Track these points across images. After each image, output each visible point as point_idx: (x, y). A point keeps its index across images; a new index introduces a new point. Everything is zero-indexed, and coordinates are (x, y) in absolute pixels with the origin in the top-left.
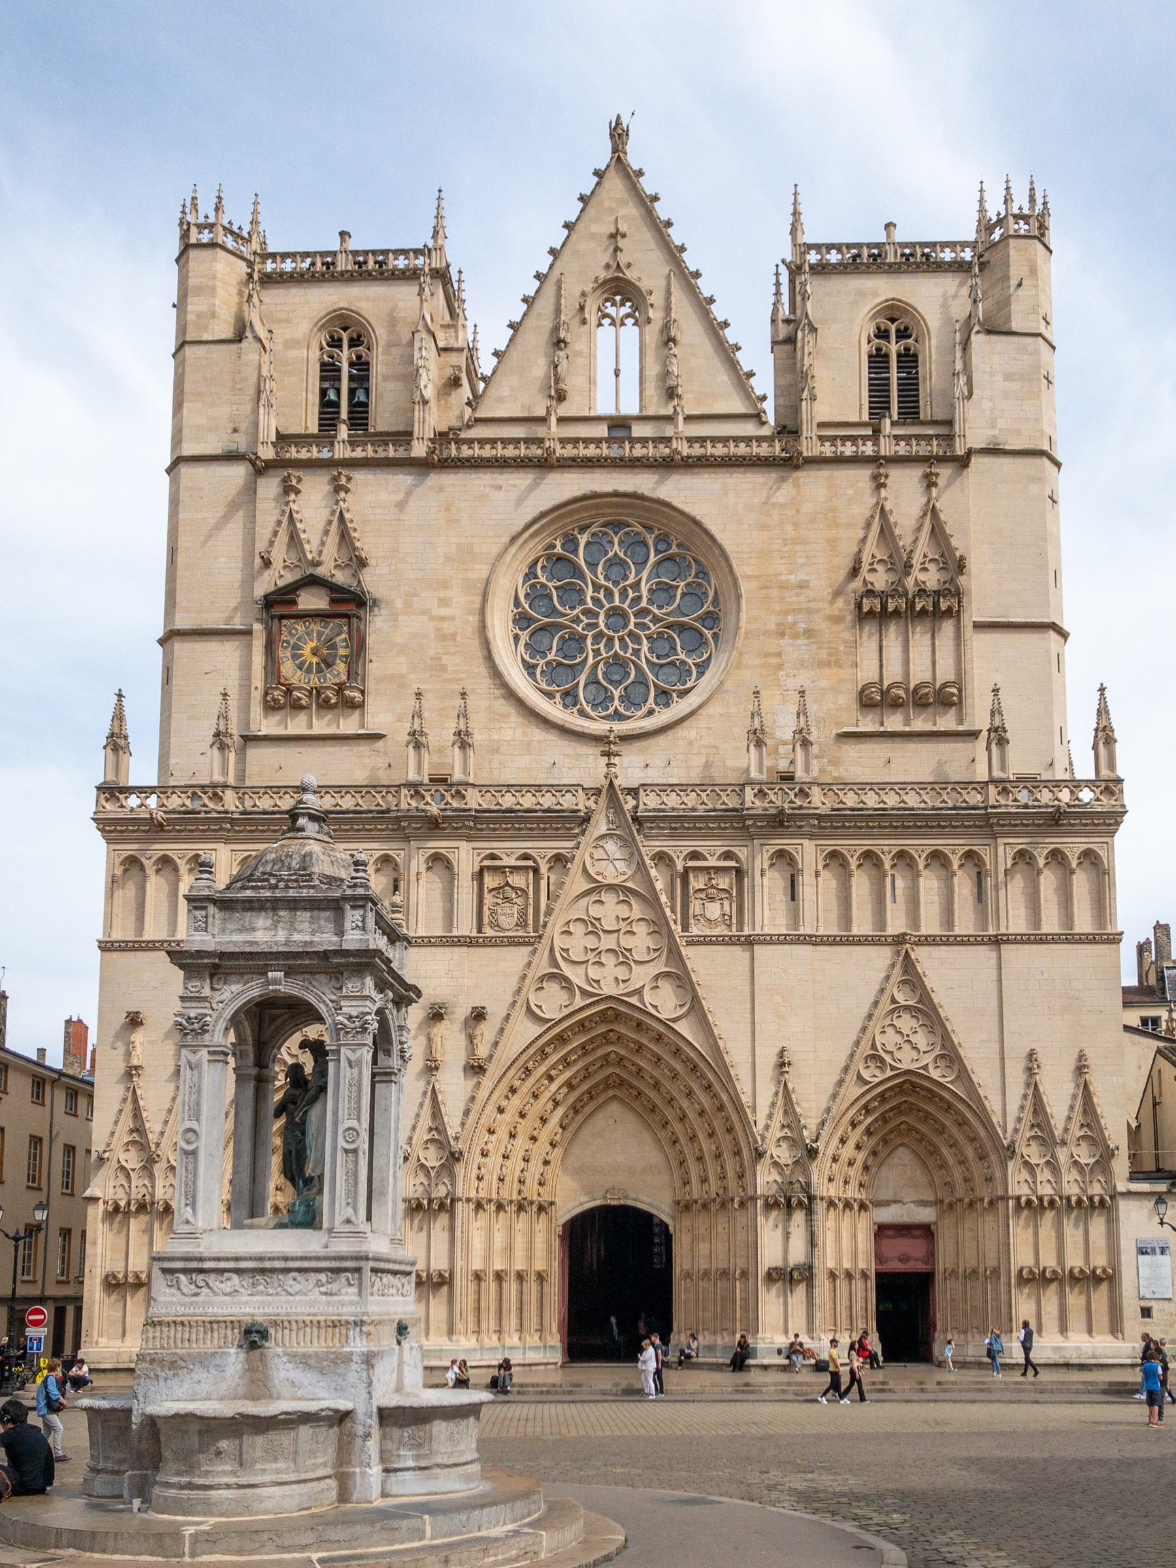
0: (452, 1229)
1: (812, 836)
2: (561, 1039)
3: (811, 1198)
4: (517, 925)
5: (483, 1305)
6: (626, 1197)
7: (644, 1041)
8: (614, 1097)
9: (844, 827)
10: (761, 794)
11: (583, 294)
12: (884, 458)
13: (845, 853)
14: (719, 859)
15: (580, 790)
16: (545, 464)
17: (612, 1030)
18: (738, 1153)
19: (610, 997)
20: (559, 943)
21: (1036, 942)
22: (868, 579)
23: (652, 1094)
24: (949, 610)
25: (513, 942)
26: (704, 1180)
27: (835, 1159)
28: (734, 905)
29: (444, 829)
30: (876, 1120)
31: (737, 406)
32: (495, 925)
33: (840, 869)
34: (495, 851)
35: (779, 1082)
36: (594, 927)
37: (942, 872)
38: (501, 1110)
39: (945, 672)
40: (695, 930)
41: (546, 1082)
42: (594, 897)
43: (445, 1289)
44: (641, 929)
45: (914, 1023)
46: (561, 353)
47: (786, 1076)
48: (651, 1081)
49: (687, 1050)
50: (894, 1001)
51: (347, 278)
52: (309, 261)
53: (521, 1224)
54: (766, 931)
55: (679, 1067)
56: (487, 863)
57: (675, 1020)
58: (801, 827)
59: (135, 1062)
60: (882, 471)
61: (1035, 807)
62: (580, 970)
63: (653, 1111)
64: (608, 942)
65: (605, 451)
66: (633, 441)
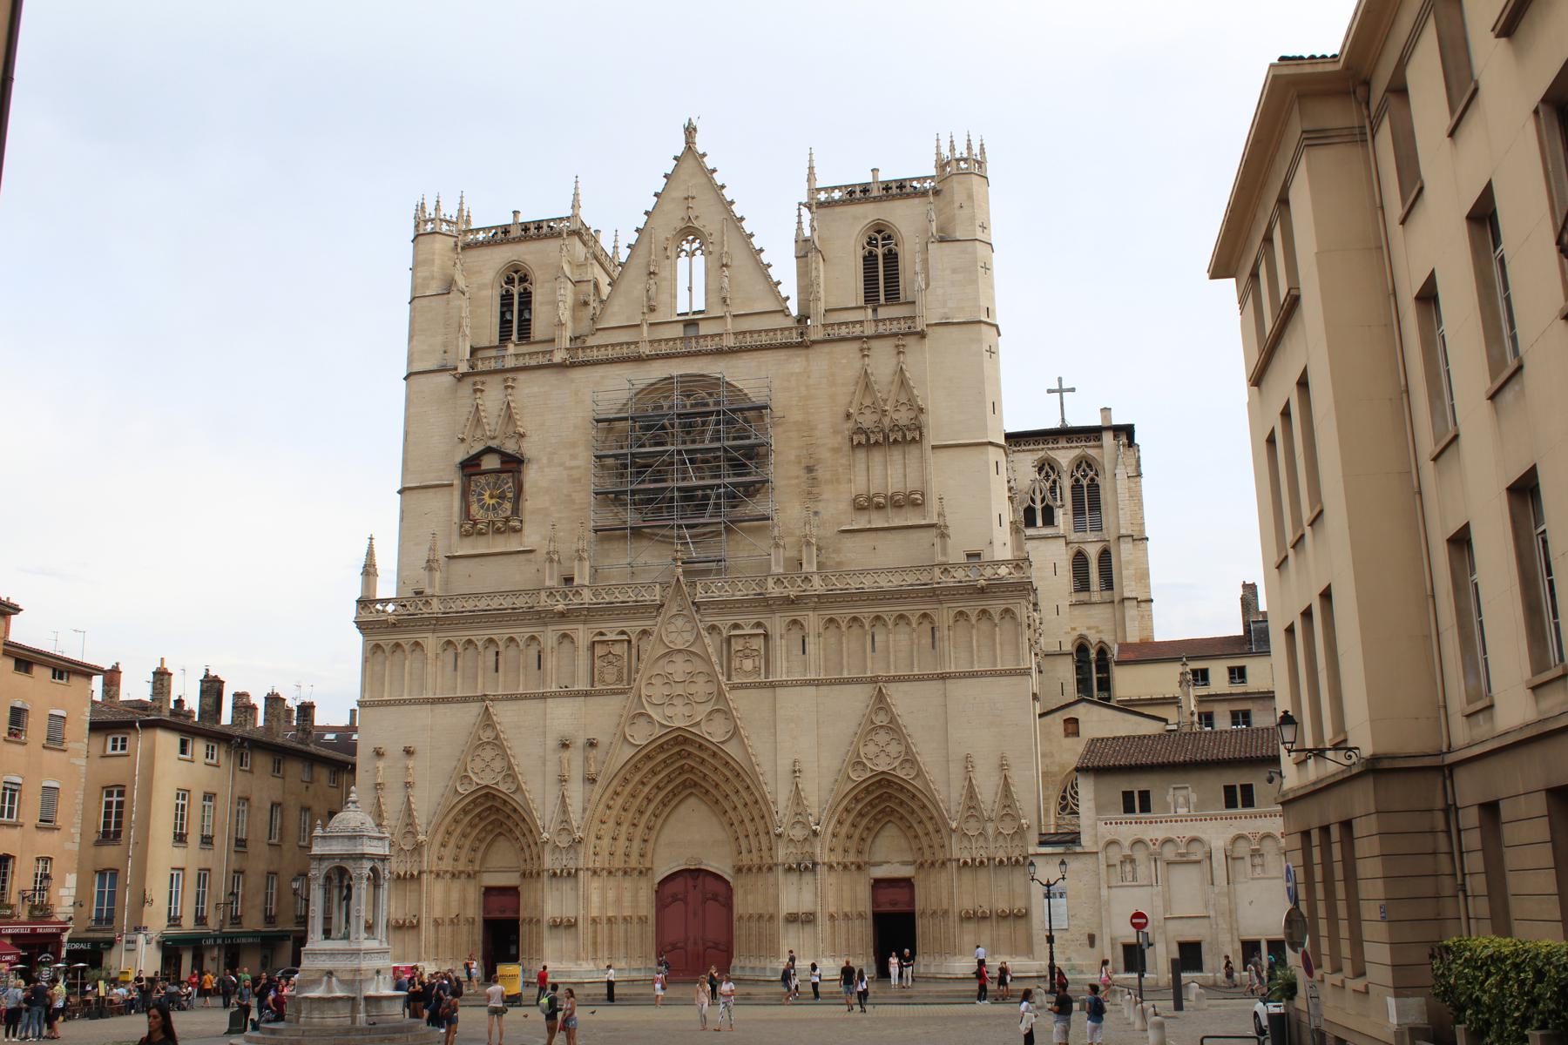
0: (577, 889)
1: (814, 609)
2: (648, 757)
3: (815, 864)
5: (599, 940)
6: (701, 863)
7: (705, 756)
8: (691, 794)
9: (836, 602)
10: (778, 581)
11: (667, 239)
12: (867, 337)
13: (838, 619)
14: (753, 627)
15: (658, 586)
16: (639, 359)
18: (768, 833)
20: (644, 692)
21: (969, 677)
22: (858, 420)
24: (914, 438)
25: (614, 693)
27: (834, 835)
30: (866, 805)
31: (771, 305)
32: (603, 681)
36: (668, 680)
37: (907, 629)
39: (913, 484)
40: (736, 680)
41: (641, 787)
42: (667, 660)
43: (573, 930)
44: (701, 680)
45: (888, 738)
46: (652, 282)
49: (732, 763)
50: (872, 722)
51: (519, 240)
52: (494, 231)
53: (627, 883)
55: (728, 774)
56: (597, 639)
57: (722, 743)
59: (379, 781)
60: (865, 346)
61: (966, 582)
62: (659, 710)
64: (679, 690)
65: (680, 348)
66: (697, 337)
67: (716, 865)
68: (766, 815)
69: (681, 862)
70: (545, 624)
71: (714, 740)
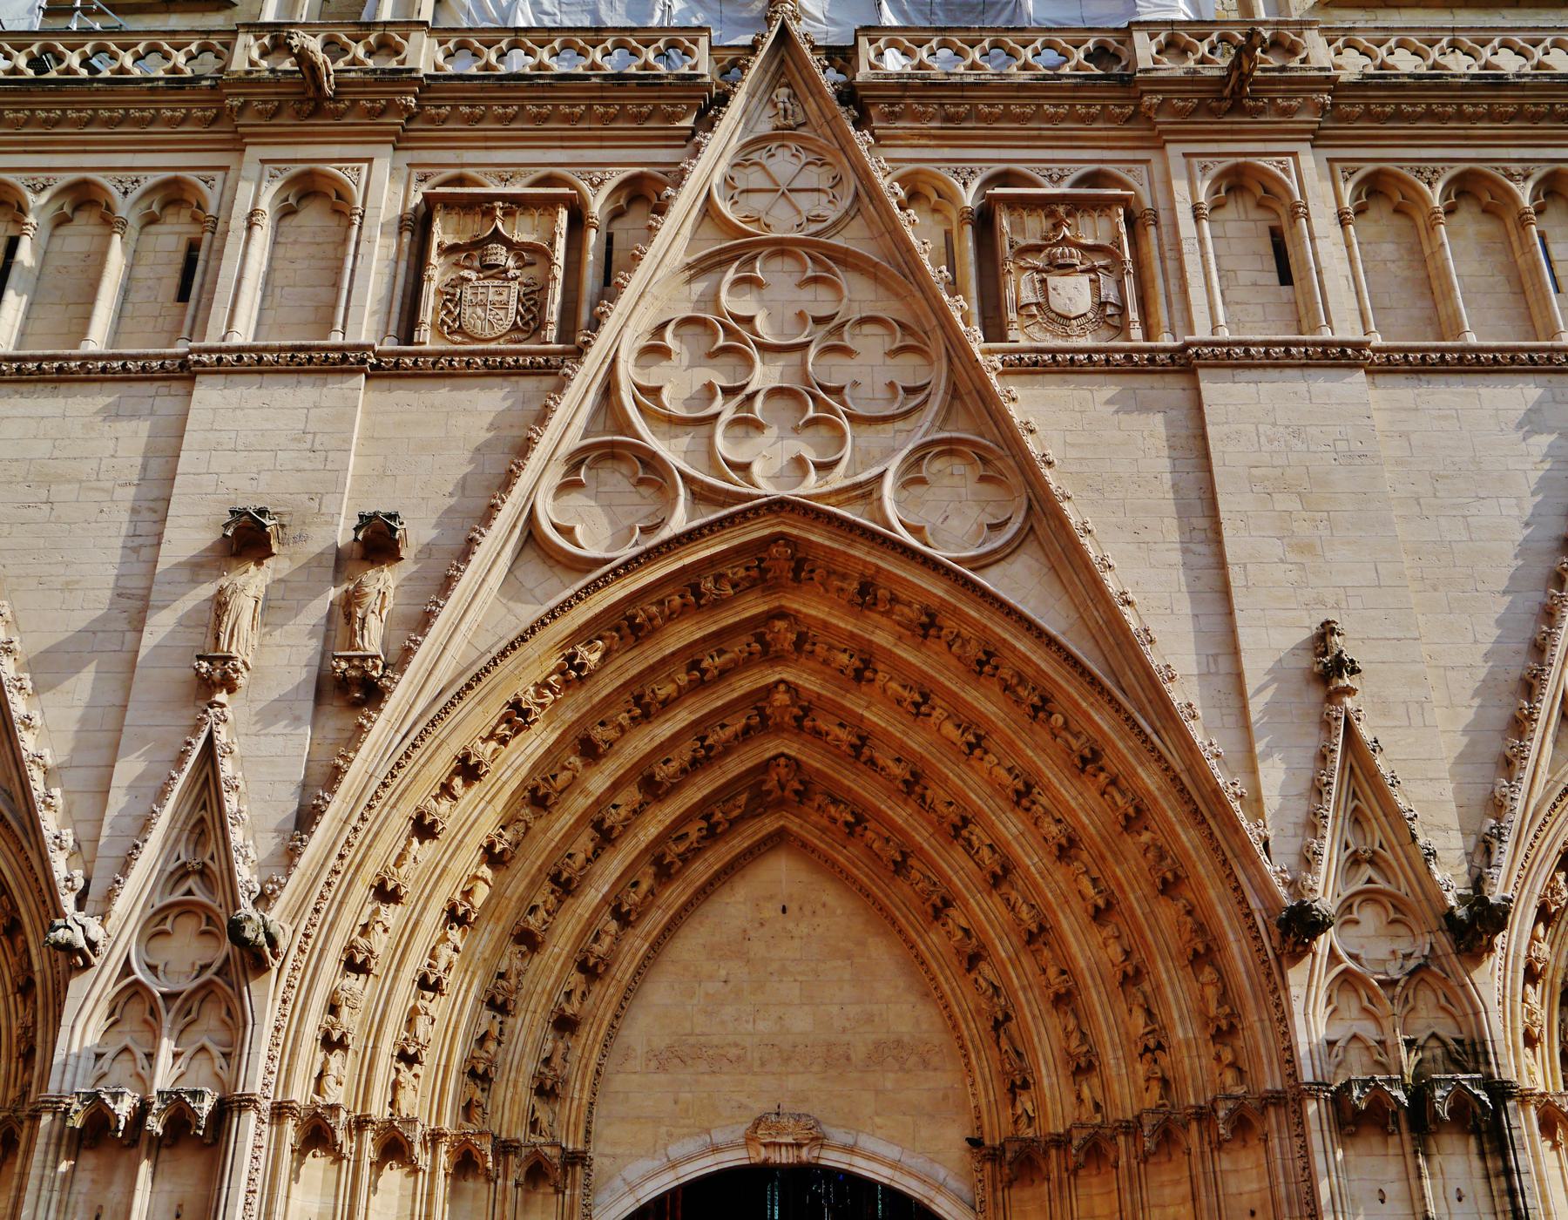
1: (1317, 139)
4: (515, 326)
6: (819, 1141)
7: (882, 638)
13: (1411, 176)
17: (780, 614)
19: (779, 506)
20: (628, 372)
23: (901, 814)
25: (497, 369)
26: (1083, 1067)
28: (1129, 283)
29: (340, 115)
33: (1400, 221)
34: (470, 172)
35: (1326, 724)
38: (423, 829)
40: (1023, 336)
41: (576, 761)
44: (871, 345)
47: (1348, 702)
48: (897, 770)
54: (1225, 334)
56: (440, 190)
57: (979, 563)
58: (1287, 112)
63: (900, 867)
67: (892, 1152)
68: (1203, 868)
69: (719, 1137)
70: (237, 145)
71: (939, 554)
